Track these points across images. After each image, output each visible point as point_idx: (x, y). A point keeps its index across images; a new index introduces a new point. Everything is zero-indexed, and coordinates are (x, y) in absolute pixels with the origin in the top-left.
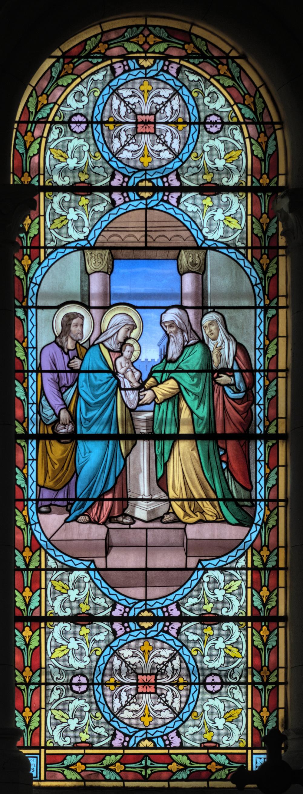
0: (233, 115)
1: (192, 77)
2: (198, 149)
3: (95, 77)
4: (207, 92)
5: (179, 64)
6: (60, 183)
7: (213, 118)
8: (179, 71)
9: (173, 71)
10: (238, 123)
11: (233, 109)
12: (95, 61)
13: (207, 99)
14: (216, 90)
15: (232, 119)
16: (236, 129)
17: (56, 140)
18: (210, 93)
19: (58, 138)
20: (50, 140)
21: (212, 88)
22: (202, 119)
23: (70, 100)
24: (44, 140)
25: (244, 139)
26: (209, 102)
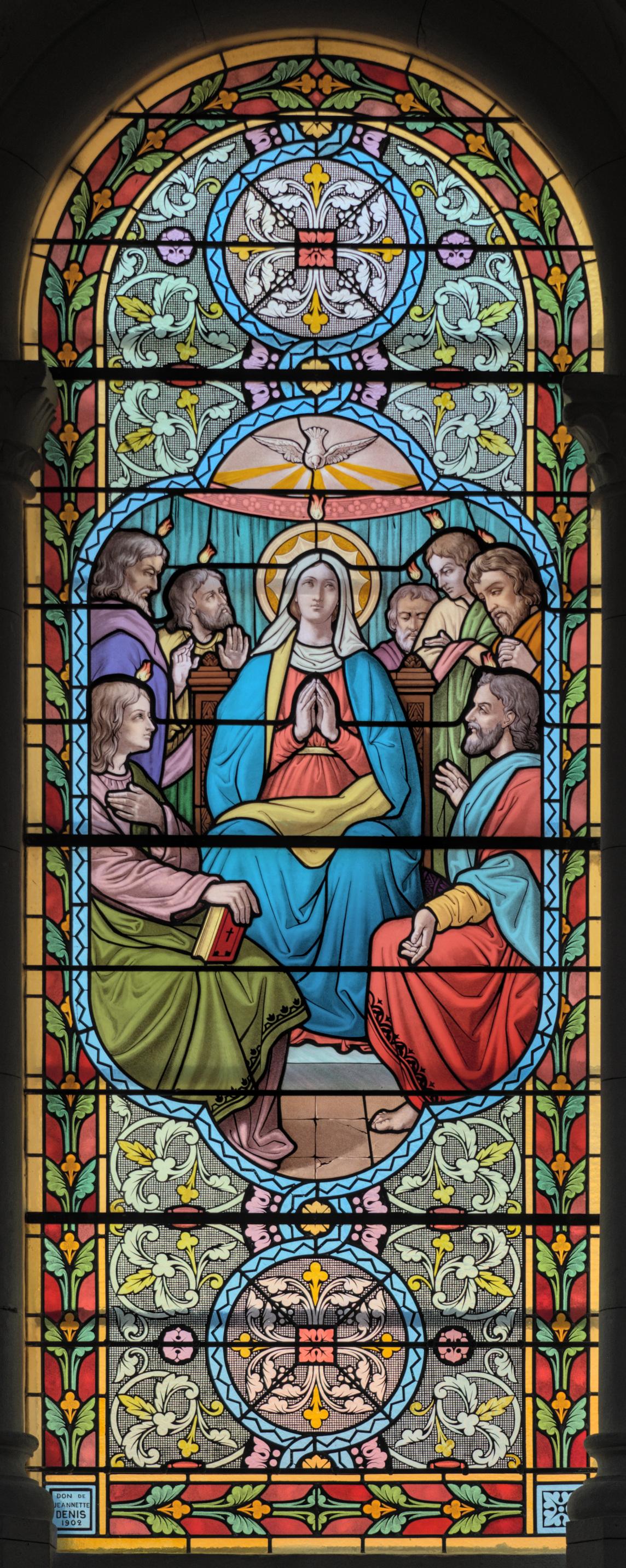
0: (498, 232)
1: (412, 158)
2: (426, 298)
3: (212, 156)
4: (441, 187)
5: (385, 131)
6: (138, 363)
7: (456, 239)
8: (384, 145)
9: (373, 147)
10: (507, 248)
11: (496, 221)
12: (210, 124)
13: (442, 201)
14: (460, 183)
15: (493, 240)
16: (503, 261)
17: (130, 278)
18: (447, 190)
19: (135, 275)
20: (117, 278)
21: (452, 180)
22: (432, 241)
23: (159, 201)
24: (105, 278)
25: (520, 279)
26: (448, 207)
